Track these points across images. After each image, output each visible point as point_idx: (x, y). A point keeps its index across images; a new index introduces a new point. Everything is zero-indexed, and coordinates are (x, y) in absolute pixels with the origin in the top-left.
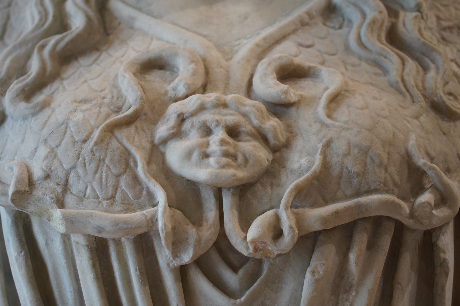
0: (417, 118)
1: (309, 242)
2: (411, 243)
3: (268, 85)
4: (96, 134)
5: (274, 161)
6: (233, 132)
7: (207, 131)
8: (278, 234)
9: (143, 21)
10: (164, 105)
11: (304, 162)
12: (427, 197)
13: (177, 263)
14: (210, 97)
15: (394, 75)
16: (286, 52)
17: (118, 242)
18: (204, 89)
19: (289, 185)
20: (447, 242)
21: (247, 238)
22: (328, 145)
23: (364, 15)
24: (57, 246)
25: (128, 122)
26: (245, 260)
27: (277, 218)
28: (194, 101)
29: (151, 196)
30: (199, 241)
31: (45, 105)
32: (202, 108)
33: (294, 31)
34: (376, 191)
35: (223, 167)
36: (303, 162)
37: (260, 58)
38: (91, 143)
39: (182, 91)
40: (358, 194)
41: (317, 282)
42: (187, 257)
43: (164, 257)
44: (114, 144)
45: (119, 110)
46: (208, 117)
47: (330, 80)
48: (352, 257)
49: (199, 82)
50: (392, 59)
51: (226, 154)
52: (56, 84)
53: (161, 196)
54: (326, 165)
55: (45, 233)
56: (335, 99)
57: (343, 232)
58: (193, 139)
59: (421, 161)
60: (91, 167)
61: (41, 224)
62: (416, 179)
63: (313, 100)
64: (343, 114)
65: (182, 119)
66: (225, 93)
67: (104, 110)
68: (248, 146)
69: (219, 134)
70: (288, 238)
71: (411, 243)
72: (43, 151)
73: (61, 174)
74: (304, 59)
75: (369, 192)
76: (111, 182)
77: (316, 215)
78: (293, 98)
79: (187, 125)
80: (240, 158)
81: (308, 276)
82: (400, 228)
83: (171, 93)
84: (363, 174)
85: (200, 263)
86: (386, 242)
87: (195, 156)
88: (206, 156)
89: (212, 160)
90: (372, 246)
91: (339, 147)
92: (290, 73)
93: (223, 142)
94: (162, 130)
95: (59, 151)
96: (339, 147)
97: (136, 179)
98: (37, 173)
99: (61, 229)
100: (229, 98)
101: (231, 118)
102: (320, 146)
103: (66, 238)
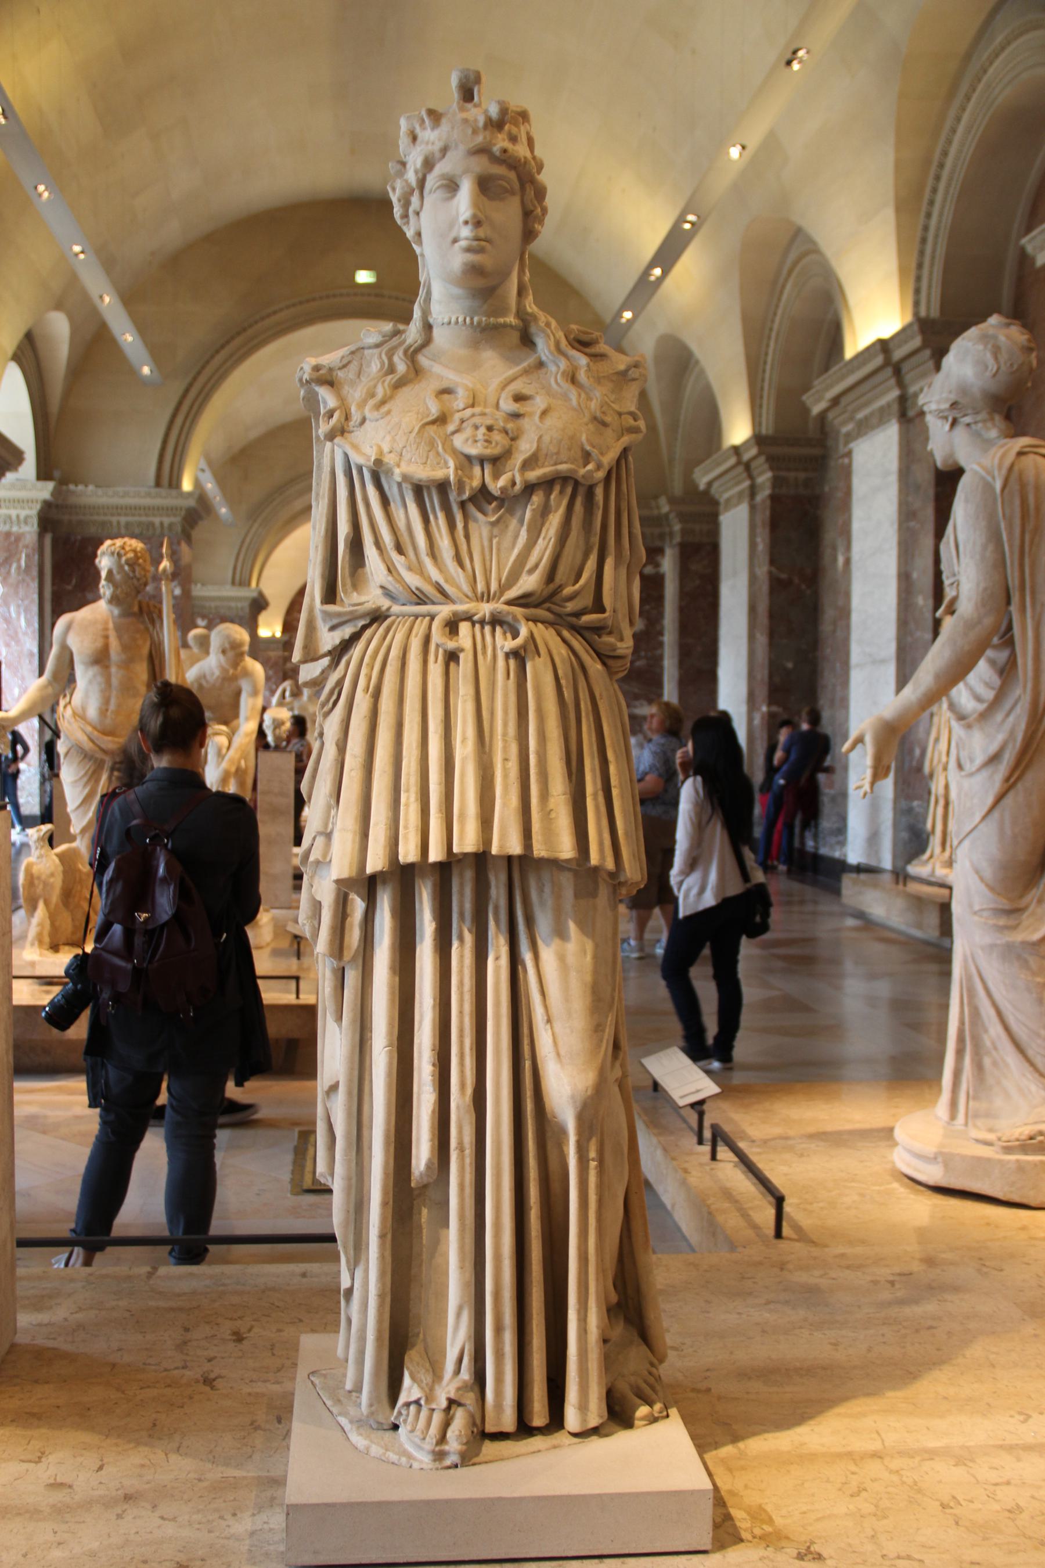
0: (587, 425)
1: (530, 489)
2: (582, 491)
3: (507, 405)
4: (416, 429)
5: (511, 446)
6: (490, 429)
7: (476, 427)
8: (514, 484)
9: (437, 369)
10: (452, 415)
11: (528, 446)
12: (590, 467)
13: (459, 499)
14: (477, 410)
15: (574, 402)
16: (518, 386)
17: (428, 488)
18: (473, 406)
19: (518, 459)
20: (599, 492)
21: (496, 486)
22: (540, 437)
23: (558, 367)
24: (395, 489)
25: (433, 422)
26: (495, 498)
27: (514, 476)
28: (469, 412)
29: (446, 463)
30: (472, 488)
31: (389, 412)
32: (473, 415)
33: (521, 375)
34: (565, 463)
35: (486, 448)
36: (525, 447)
37: (503, 388)
38: (414, 434)
39: (461, 406)
40: (556, 464)
41: (534, 510)
42: (466, 495)
43: (453, 497)
44: (426, 435)
45: (428, 416)
46: (477, 420)
47: (540, 403)
48: (552, 497)
49: (471, 402)
50: (573, 394)
51: (486, 441)
52: (392, 402)
53: (451, 464)
54: (538, 448)
55: (389, 483)
56: (544, 413)
57: (548, 484)
58: (468, 432)
59: (588, 448)
60: (414, 447)
61: (386, 477)
62: (587, 457)
63: (531, 415)
64: (549, 421)
65: (462, 421)
66: (485, 407)
67: (420, 417)
68: (497, 437)
69: (482, 430)
70: (518, 487)
71: (582, 491)
72: (388, 438)
73: (399, 450)
74: (526, 391)
75: (561, 463)
76: (425, 455)
77: (533, 475)
78: (522, 412)
79: (465, 425)
80: (494, 444)
81: (529, 507)
82: (577, 484)
83: (455, 408)
84: (558, 453)
85: (472, 499)
86: (569, 490)
87: (470, 442)
88: (476, 441)
89: (479, 444)
90: (561, 492)
91: (546, 439)
92: (519, 398)
93: (484, 435)
94: (451, 427)
95: (397, 438)
96: (546, 439)
97: (438, 453)
98: (386, 449)
99: (399, 479)
100: (487, 411)
101: (489, 422)
102: (536, 438)
103: (399, 485)
